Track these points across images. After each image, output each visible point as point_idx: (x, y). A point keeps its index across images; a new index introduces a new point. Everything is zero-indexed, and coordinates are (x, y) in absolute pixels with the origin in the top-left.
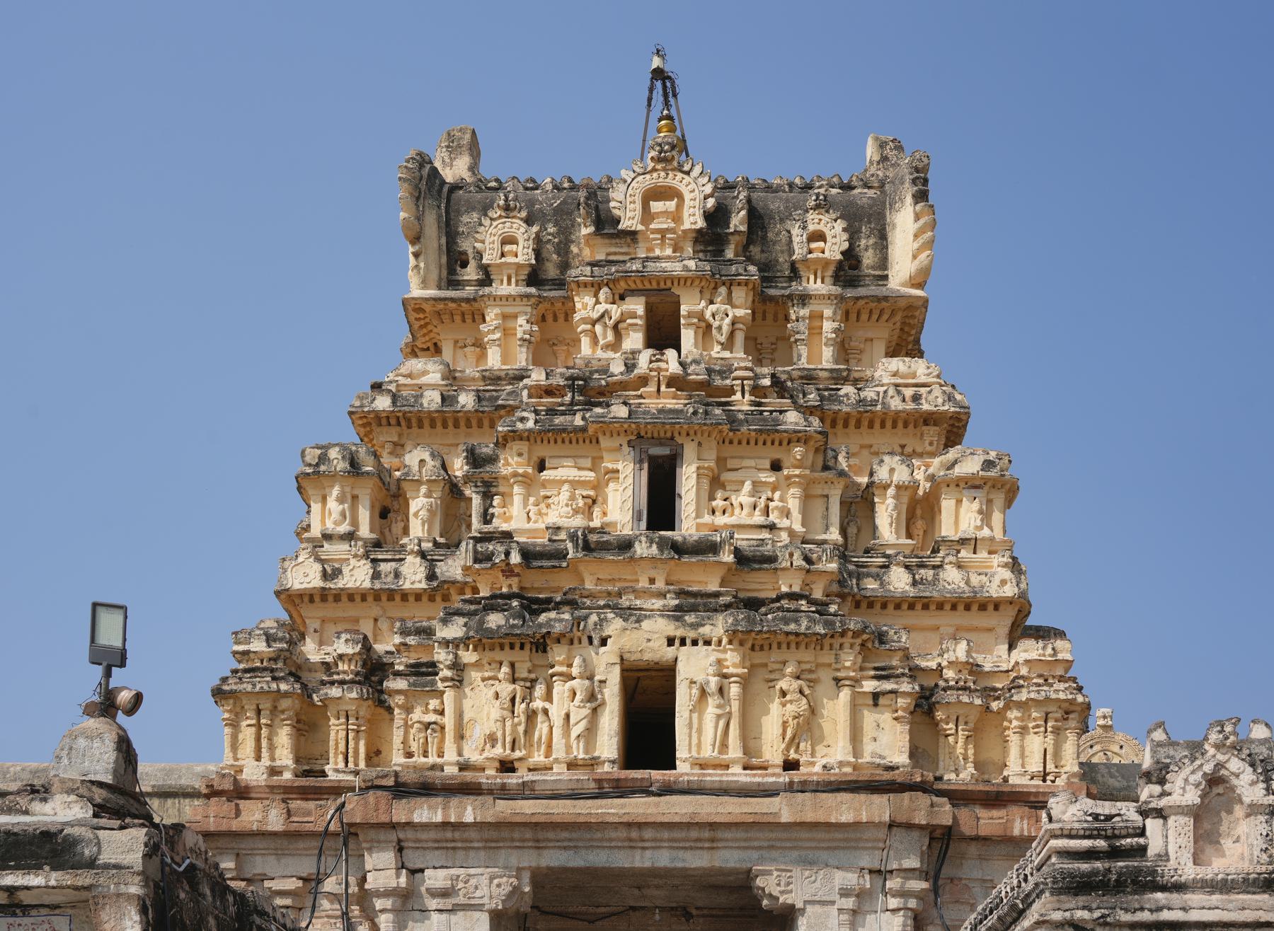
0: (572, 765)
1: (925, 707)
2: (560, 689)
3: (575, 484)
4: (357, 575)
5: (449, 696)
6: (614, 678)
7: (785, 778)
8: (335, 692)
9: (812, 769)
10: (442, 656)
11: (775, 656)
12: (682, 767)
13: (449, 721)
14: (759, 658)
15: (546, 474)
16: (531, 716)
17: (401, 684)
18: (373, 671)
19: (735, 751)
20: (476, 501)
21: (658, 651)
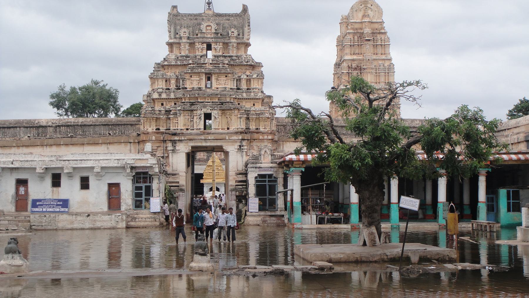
0: (197, 129)
1: (248, 119)
2: (195, 118)
3: (196, 80)
4: (164, 96)
5: (179, 118)
6: (203, 116)
7: (227, 131)
8: (162, 117)
9: (232, 129)
10: (178, 112)
11: (226, 112)
12: (213, 130)
13: (179, 122)
14: (223, 112)
15: (192, 79)
16: (191, 121)
17: (172, 116)
18: (168, 112)
19: (220, 127)
20: (181, 81)
21: (209, 111)
